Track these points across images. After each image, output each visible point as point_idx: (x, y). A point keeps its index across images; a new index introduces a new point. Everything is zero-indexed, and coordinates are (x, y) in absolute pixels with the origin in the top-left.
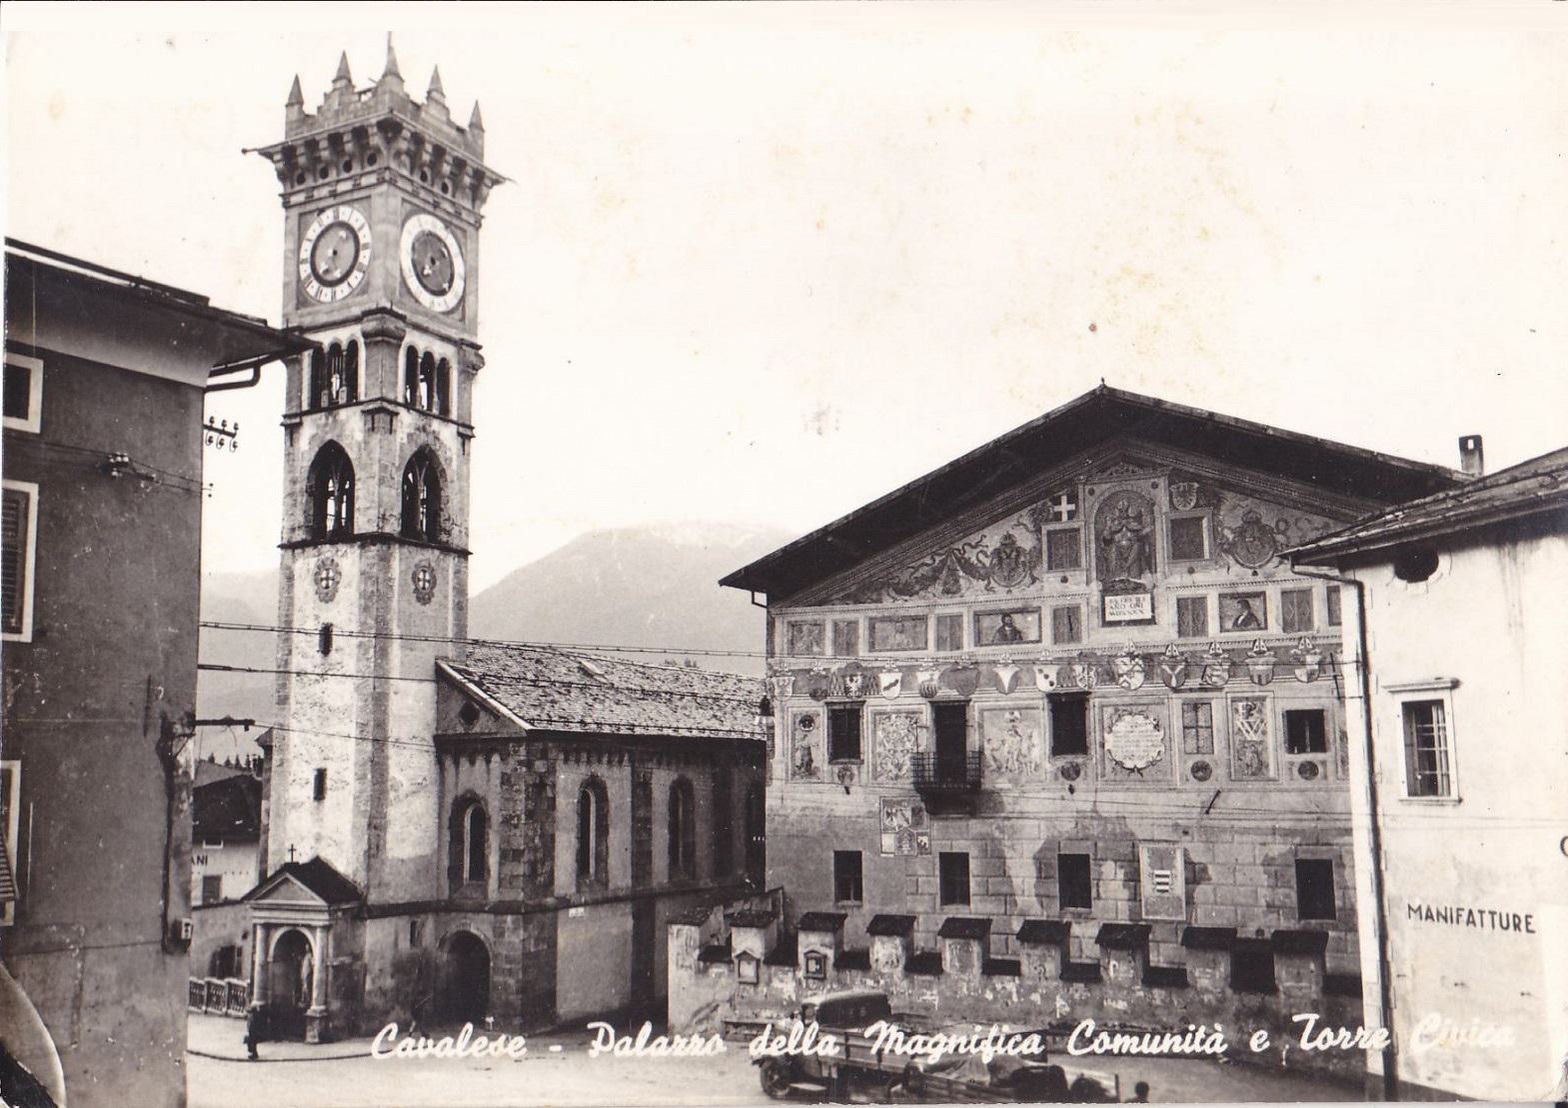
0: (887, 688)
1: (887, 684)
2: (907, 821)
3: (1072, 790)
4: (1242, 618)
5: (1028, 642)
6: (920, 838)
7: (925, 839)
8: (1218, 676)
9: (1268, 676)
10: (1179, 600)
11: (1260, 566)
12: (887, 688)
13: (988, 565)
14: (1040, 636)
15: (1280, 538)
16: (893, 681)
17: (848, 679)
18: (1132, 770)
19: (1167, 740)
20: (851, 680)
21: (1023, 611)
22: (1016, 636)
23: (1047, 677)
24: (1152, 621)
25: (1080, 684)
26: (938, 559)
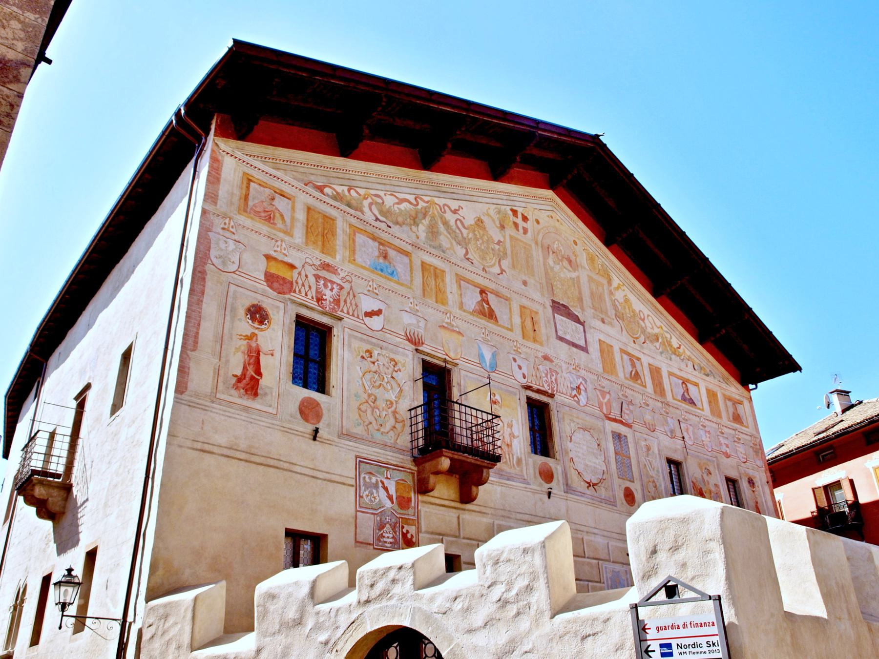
0: (369, 314)
1: (369, 310)
2: (390, 498)
3: (549, 494)
4: (633, 373)
5: (503, 327)
6: (406, 528)
7: (412, 530)
8: (627, 414)
9: (652, 425)
10: (600, 340)
11: (637, 338)
12: (369, 314)
13: (465, 235)
14: (512, 325)
15: (641, 322)
16: (376, 309)
17: (322, 282)
18: (589, 484)
19: (606, 461)
20: (325, 286)
21: (497, 294)
22: (491, 315)
23: (520, 368)
24: (585, 349)
25: (546, 386)
26: (422, 204)
